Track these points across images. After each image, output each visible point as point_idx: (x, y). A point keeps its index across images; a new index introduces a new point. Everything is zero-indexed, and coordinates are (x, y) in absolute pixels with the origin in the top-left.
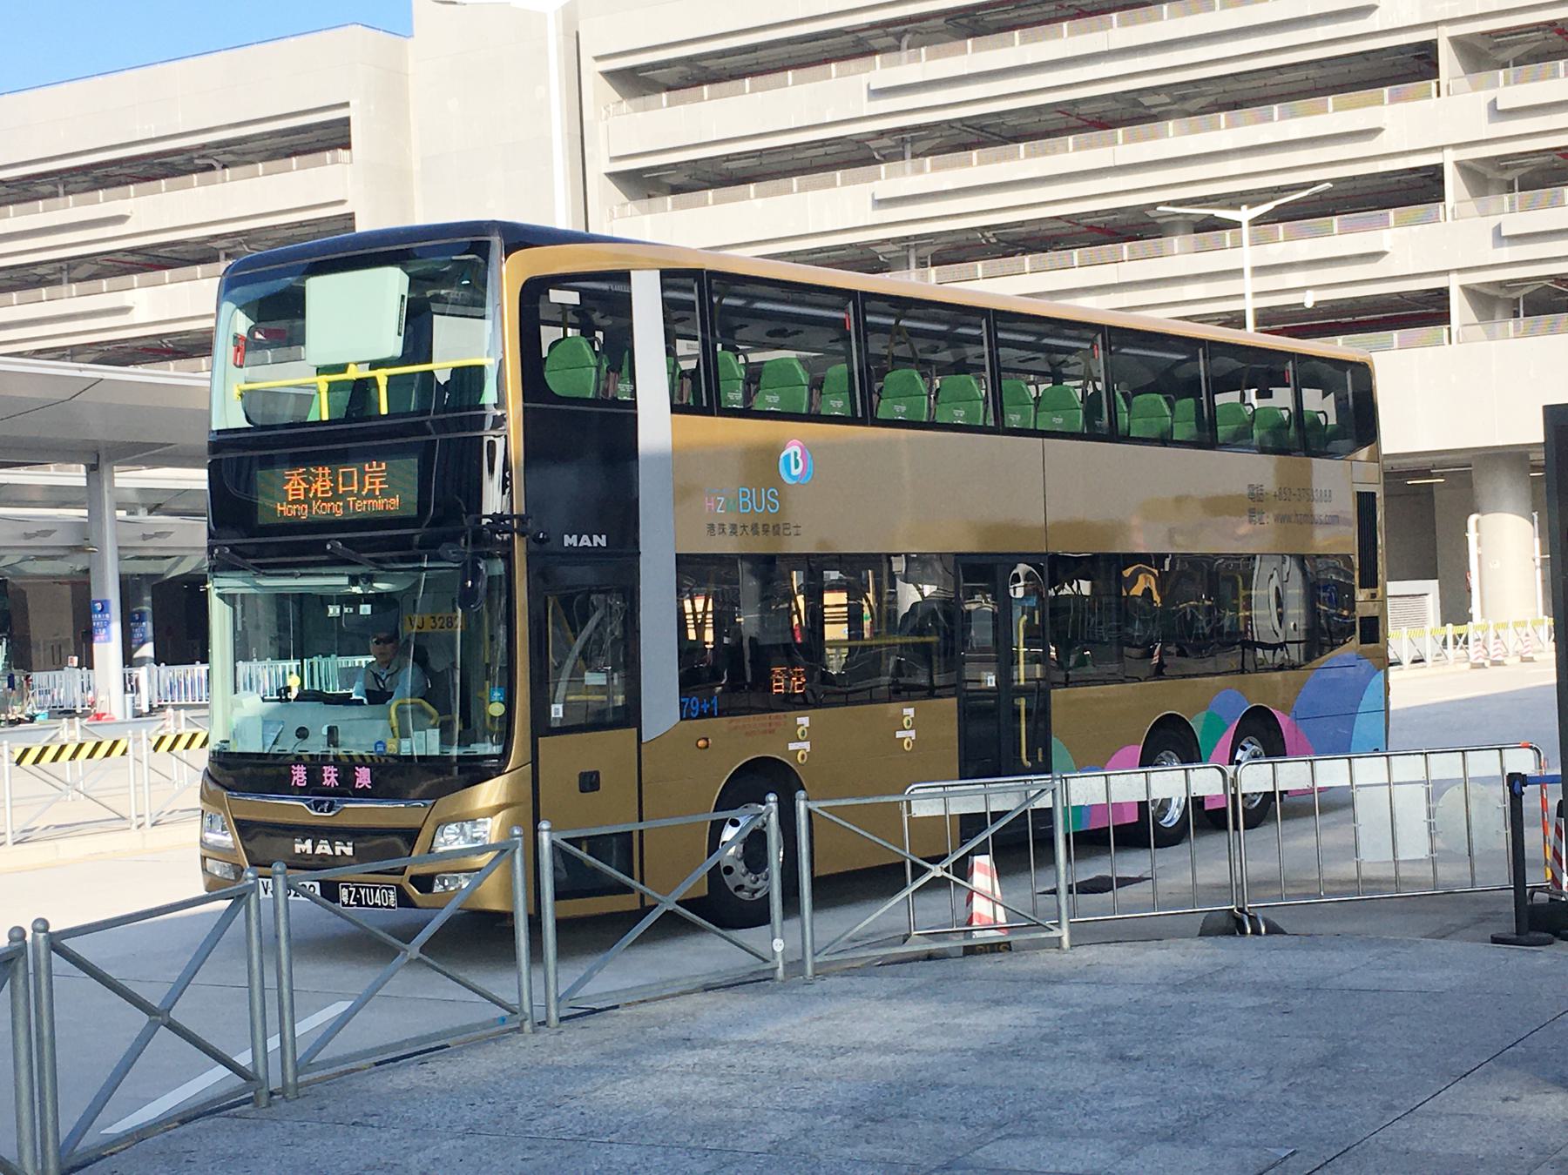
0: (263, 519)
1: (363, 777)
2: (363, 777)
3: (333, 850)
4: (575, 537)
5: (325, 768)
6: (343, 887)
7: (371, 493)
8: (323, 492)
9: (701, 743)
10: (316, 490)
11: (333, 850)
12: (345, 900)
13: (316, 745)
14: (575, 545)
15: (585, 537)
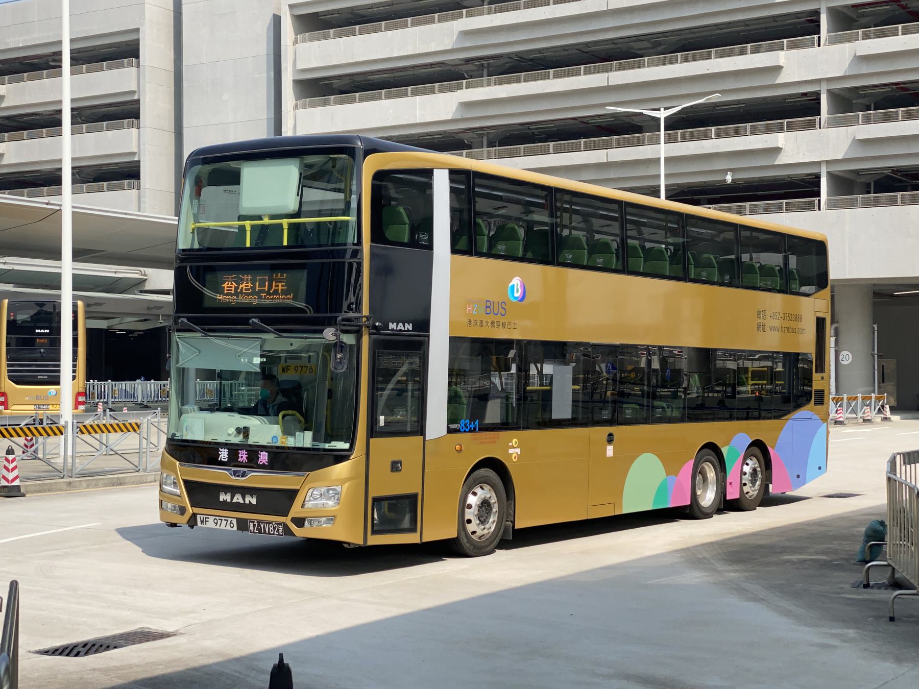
0: (207, 304)
1: (264, 457)
2: (264, 457)
3: (244, 501)
4: (395, 324)
5: (239, 451)
6: (250, 522)
7: (276, 292)
8: (246, 290)
9: (458, 447)
10: (242, 288)
11: (244, 499)
12: (252, 529)
13: (238, 439)
14: (395, 329)
15: (401, 324)
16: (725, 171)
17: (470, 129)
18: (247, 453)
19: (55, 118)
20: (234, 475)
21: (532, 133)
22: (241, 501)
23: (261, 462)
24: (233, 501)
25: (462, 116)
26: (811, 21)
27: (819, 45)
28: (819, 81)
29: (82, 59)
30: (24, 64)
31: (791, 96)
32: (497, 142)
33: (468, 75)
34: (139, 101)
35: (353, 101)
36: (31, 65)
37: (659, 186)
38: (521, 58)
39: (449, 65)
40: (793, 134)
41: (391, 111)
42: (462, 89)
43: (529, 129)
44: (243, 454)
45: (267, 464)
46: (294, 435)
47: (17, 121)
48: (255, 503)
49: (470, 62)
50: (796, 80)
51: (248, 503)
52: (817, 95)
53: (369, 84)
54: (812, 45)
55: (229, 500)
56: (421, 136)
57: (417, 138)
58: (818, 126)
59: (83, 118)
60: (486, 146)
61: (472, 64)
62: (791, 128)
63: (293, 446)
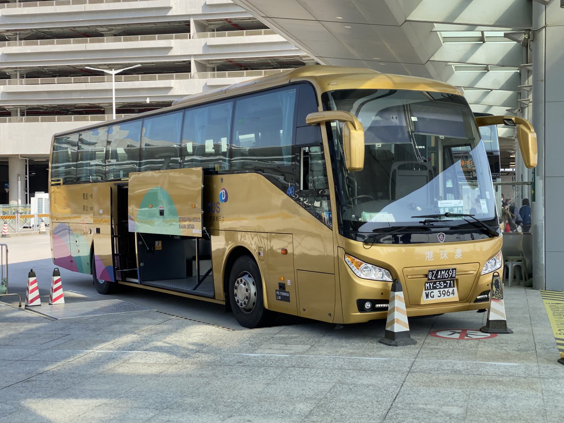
16: (146, 97)
17: (9, 68)
21: (45, 71)
26: (187, 25)
27: (190, 38)
28: (190, 56)
31: (177, 62)
37: (112, 103)
38: (38, 31)
40: (178, 81)
43: (44, 69)
50: (179, 54)
52: (189, 63)
54: (187, 38)
58: (190, 77)
62: (177, 78)
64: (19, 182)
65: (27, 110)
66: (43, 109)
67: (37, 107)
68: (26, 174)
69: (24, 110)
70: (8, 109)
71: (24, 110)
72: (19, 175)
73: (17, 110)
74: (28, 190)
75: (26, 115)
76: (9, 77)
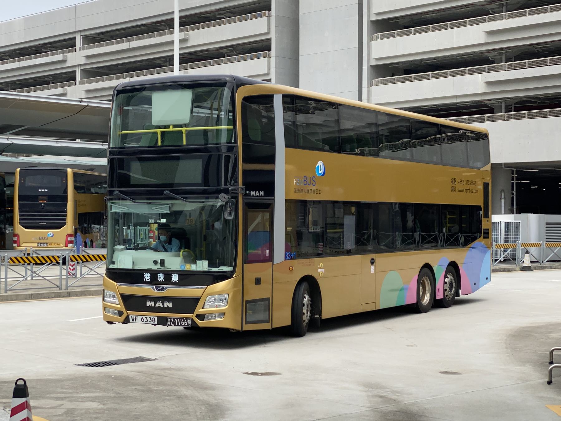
1: (175, 278)
2: (175, 278)
5: (158, 274)
11: (163, 305)
17: (492, 50)
18: (163, 275)
19: (220, 52)
20: (156, 290)
21: (537, 50)
22: (161, 306)
23: (173, 280)
24: (156, 306)
25: (485, 41)
29: (237, 12)
30: (201, 18)
32: (513, 58)
33: (492, 12)
34: (271, 39)
35: (410, 33)
36: (206, 17)
39: (478, 5)
41: (436, 40)
42: (485, 22)
43: (536, 48)
44: (161, 276)
45: (178, 281)
46: (195, 263)
47: (198, 55)
48: (171, 307)
49: (493, 2)
51: (166, 306)
53: (425, 21)
55: (153, 305)
56: (458, 56)
57: (455, 57)
59: (237, 52)
60: (505, 62)
61: (494, 4)
63: (195, 270)
64: (503, 200)
65: (515, 104)
66: (536, 102)
67: (524, 99)
68: (513, 190)
69: (512, 105)
70: (491, 104)
71: (512, 105)
72: (502, 190)
73: (501, 106)
74: (515, 210)
75: (513, 110)
76: (493, 62)
